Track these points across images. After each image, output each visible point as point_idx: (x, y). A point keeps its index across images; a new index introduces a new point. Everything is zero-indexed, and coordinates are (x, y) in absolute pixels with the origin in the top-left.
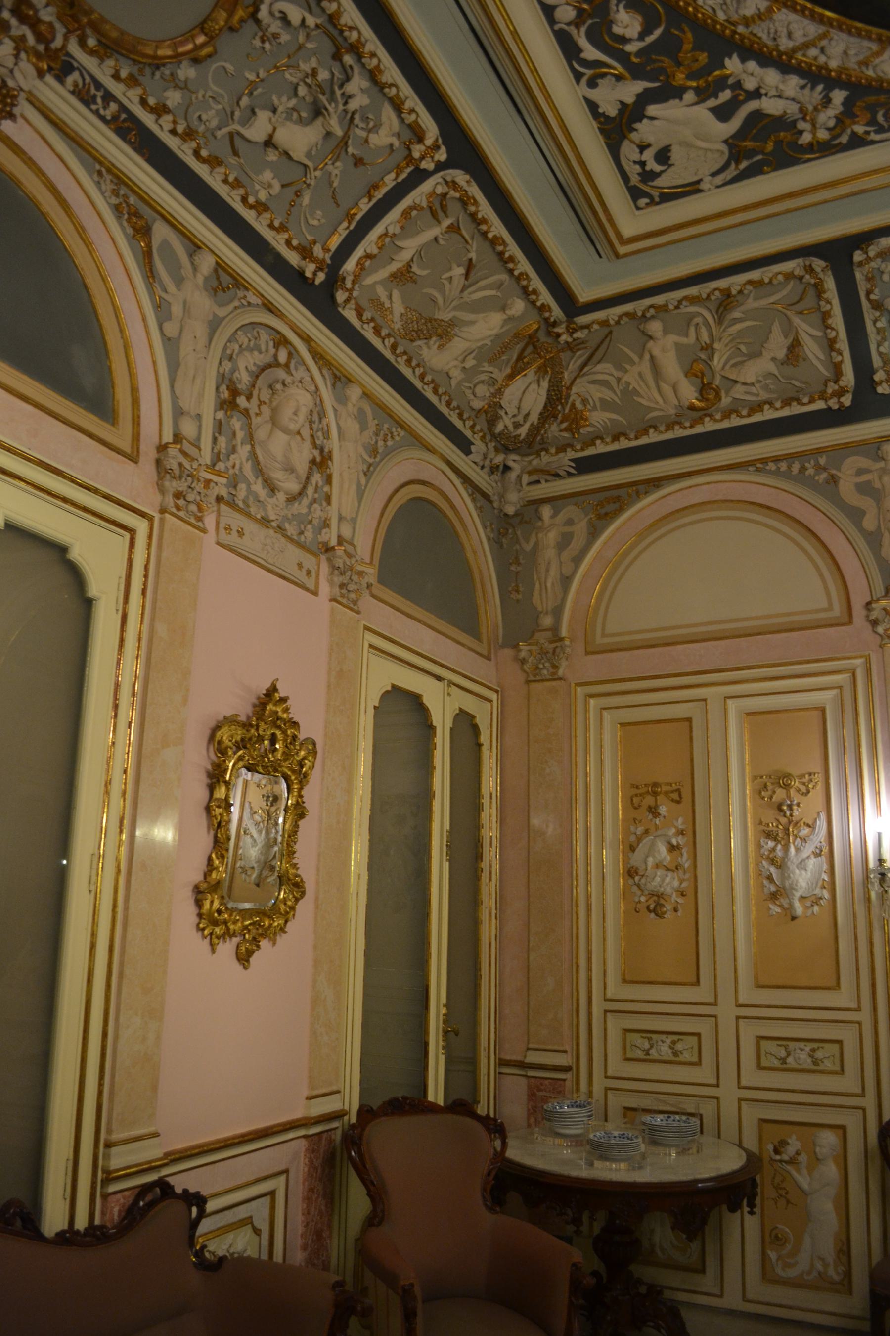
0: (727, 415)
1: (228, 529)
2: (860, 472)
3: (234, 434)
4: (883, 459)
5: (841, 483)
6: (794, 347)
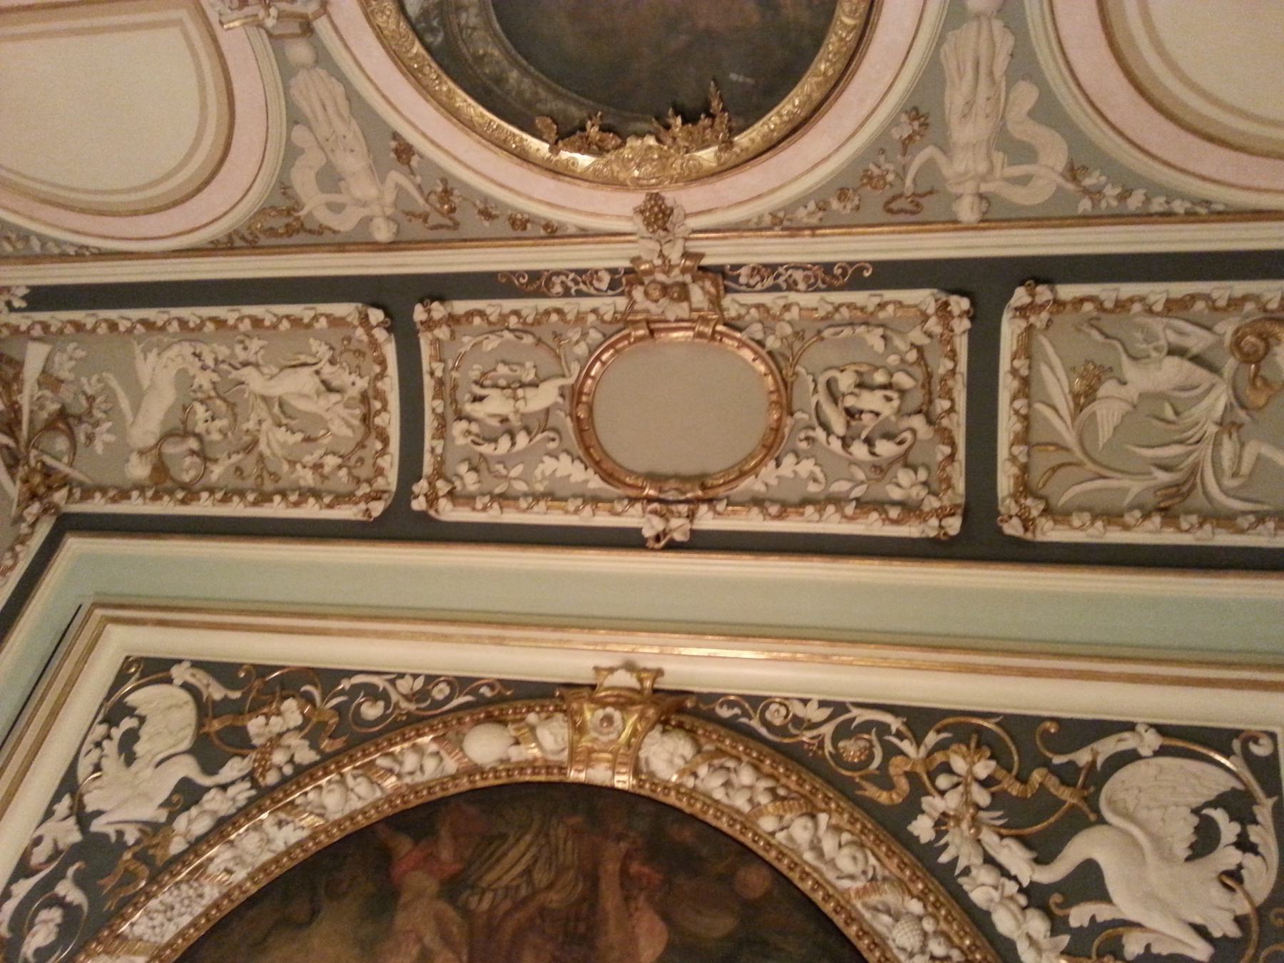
0: (1235, 304)
2: (1024, 180)
4: (981, 196)
5: (1061, 164)
6: (1084, 398)
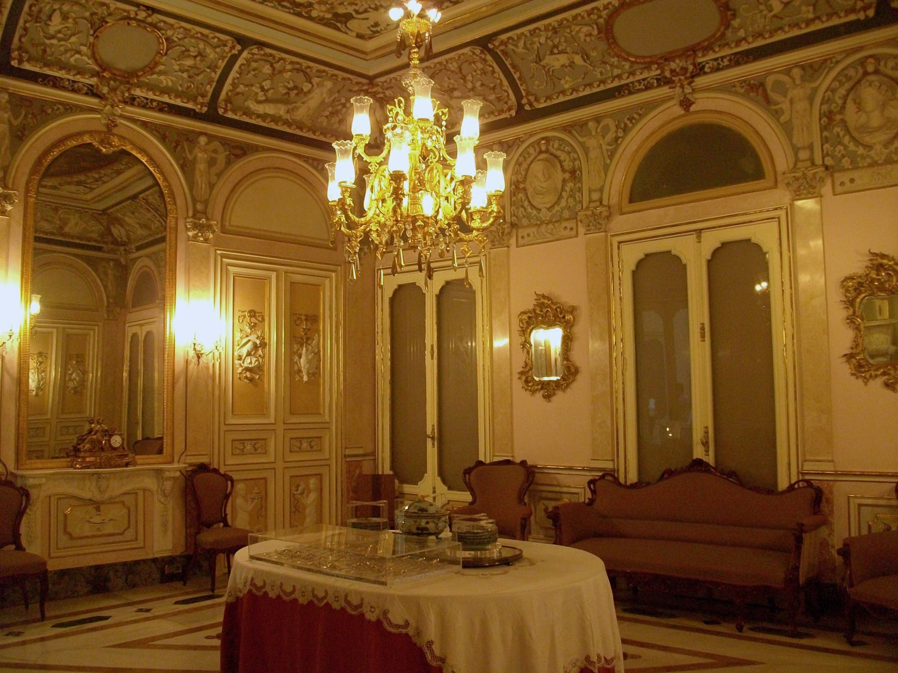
1: (842, 184)
3: (838, 135)
